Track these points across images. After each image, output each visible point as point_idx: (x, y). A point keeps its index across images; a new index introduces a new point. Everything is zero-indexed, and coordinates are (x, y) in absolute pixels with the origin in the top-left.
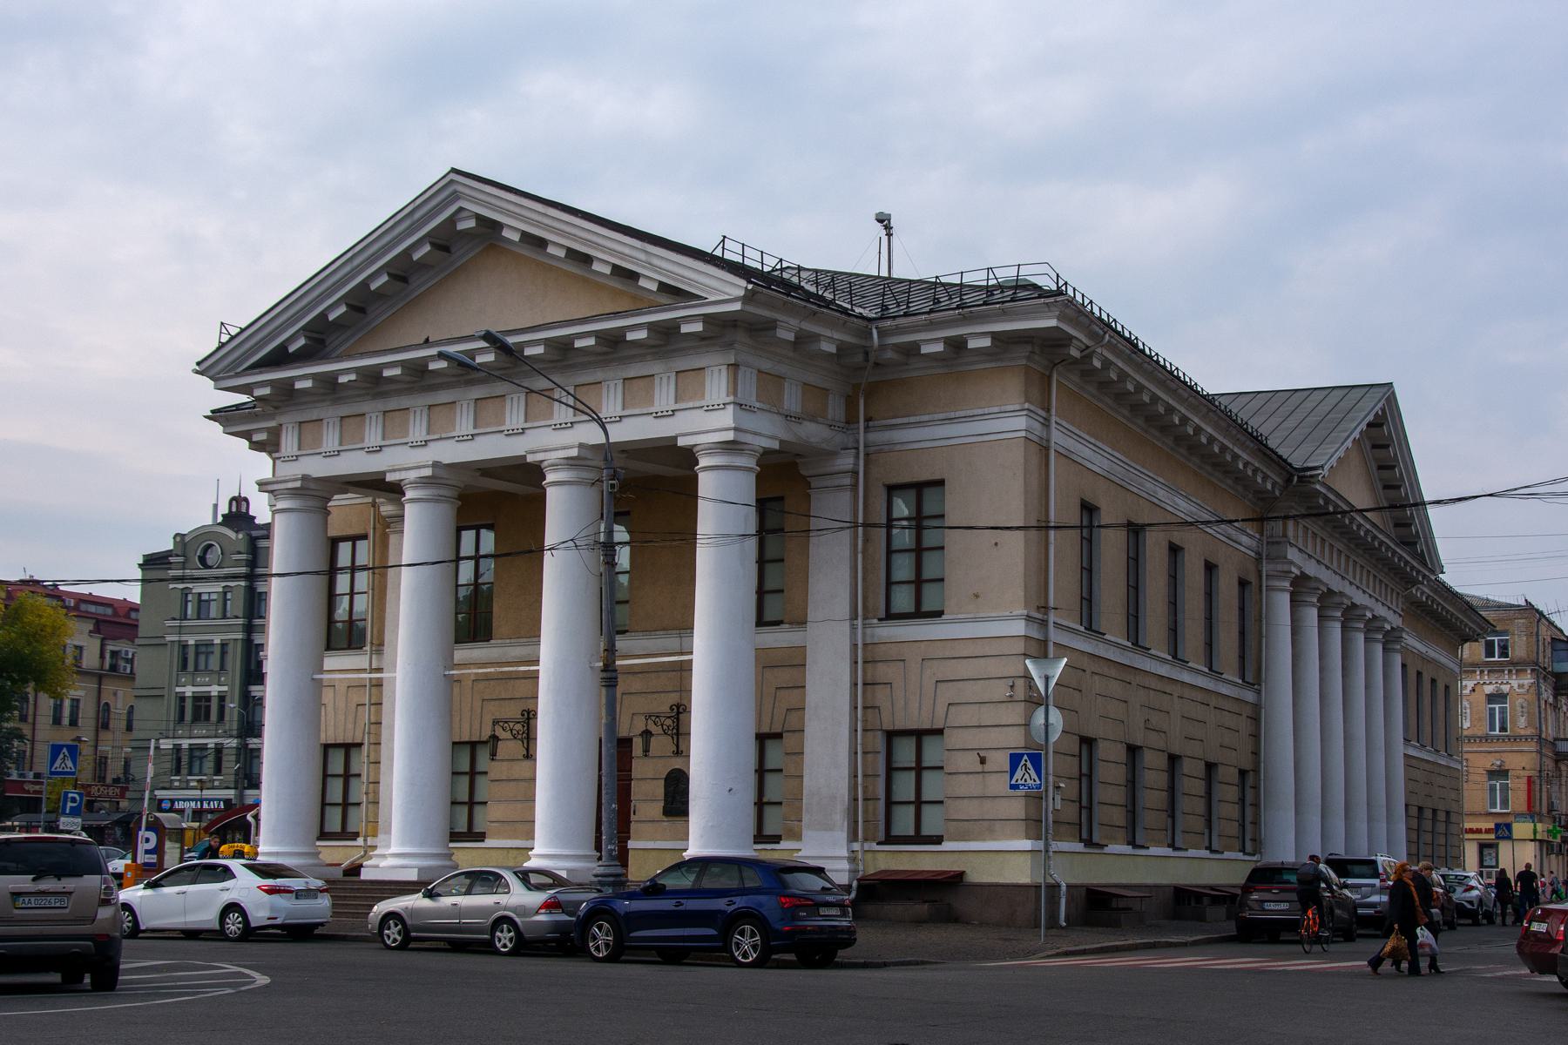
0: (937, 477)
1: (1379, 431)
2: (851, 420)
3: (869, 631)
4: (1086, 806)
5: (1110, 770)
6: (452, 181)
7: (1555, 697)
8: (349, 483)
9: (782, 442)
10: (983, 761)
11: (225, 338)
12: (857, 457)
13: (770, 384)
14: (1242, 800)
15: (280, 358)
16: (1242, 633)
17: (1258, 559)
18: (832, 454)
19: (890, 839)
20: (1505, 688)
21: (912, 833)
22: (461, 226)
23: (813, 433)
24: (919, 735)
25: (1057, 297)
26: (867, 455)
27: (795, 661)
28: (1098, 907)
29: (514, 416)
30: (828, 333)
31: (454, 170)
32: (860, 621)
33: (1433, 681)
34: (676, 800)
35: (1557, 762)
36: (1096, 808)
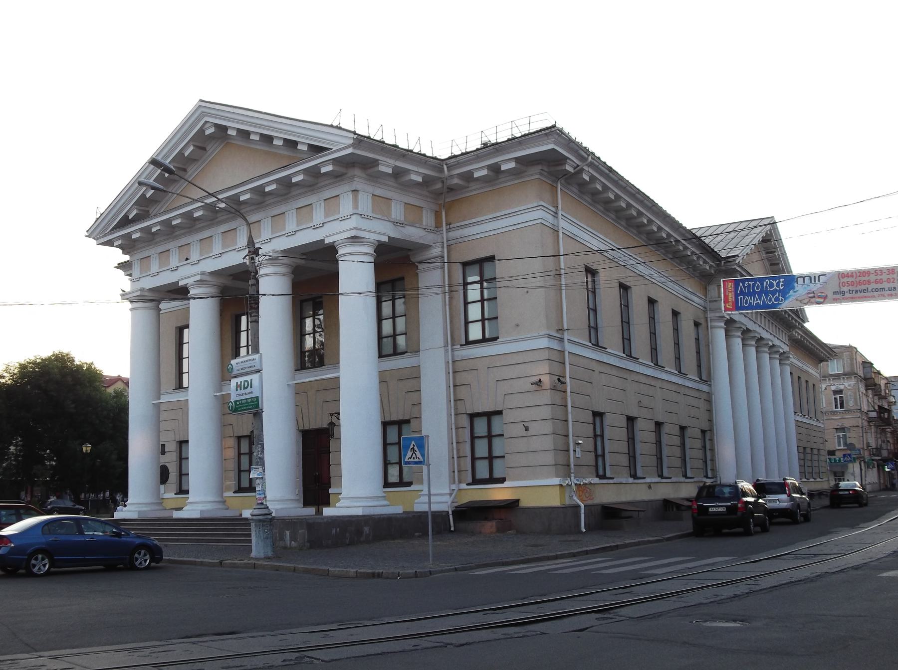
0: (491, 254)
1: (769, 245)
2: (438, 225)
3: (456, 353)
4: (599, 456)
5: (615, 430)
7: (866, 390)
8: (169, 291)
9: (389, 238)
10: (527, 429)
11: (98, 215)
12: (443, 247)
13: (381, 204)
14: (704, 447)
15: (125, 222)
16: (698, 353)
17: (705, 311)
18: (427, 247)
19: (475, 481)
20: (842, 387)
21: (488, 477)
22: (207, 132)
23: (413, 234)
24: (489, 415)
25: (553, 132)
26: (448, 246)
27: (415, 375)
28: (609, 516)
30: (415, 169)
32: (450, 347)
33: (807, 381)
35: (869, 422)
36: (607, 456)
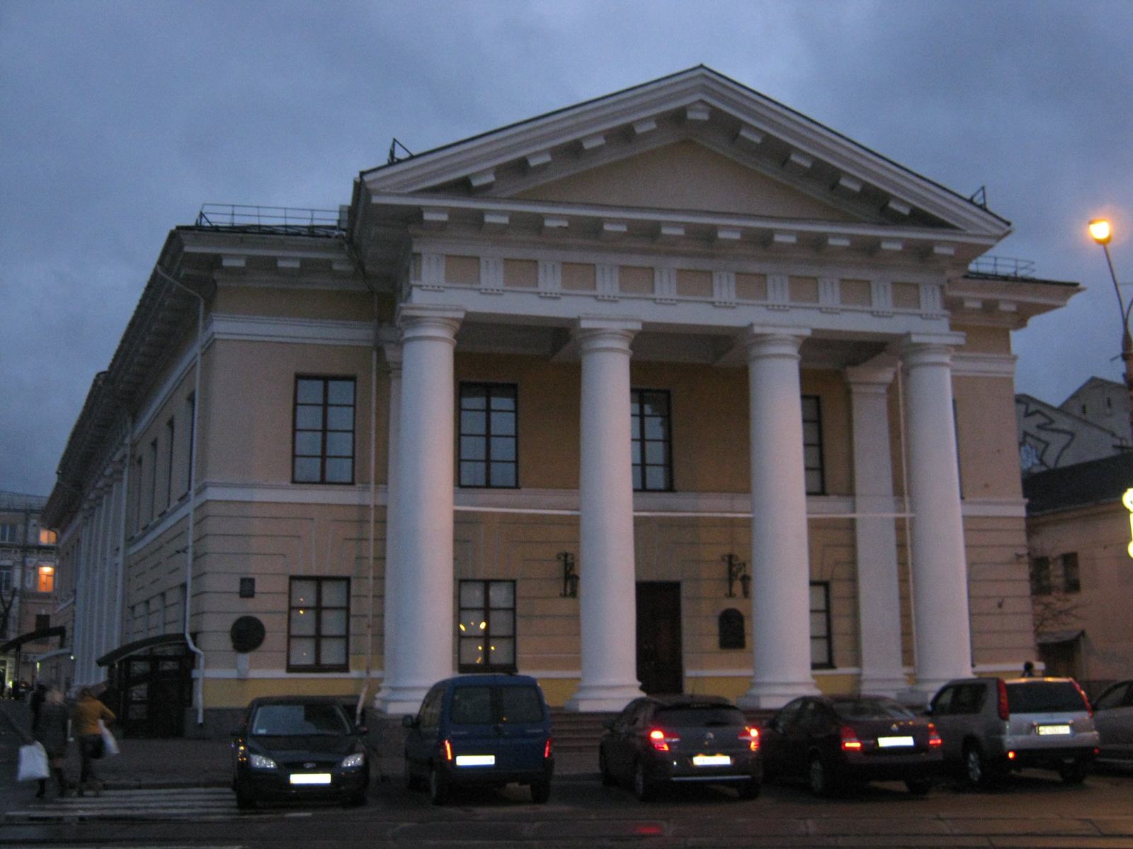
29: (725, 290)
31: (702, 66)
34: (733, 631)
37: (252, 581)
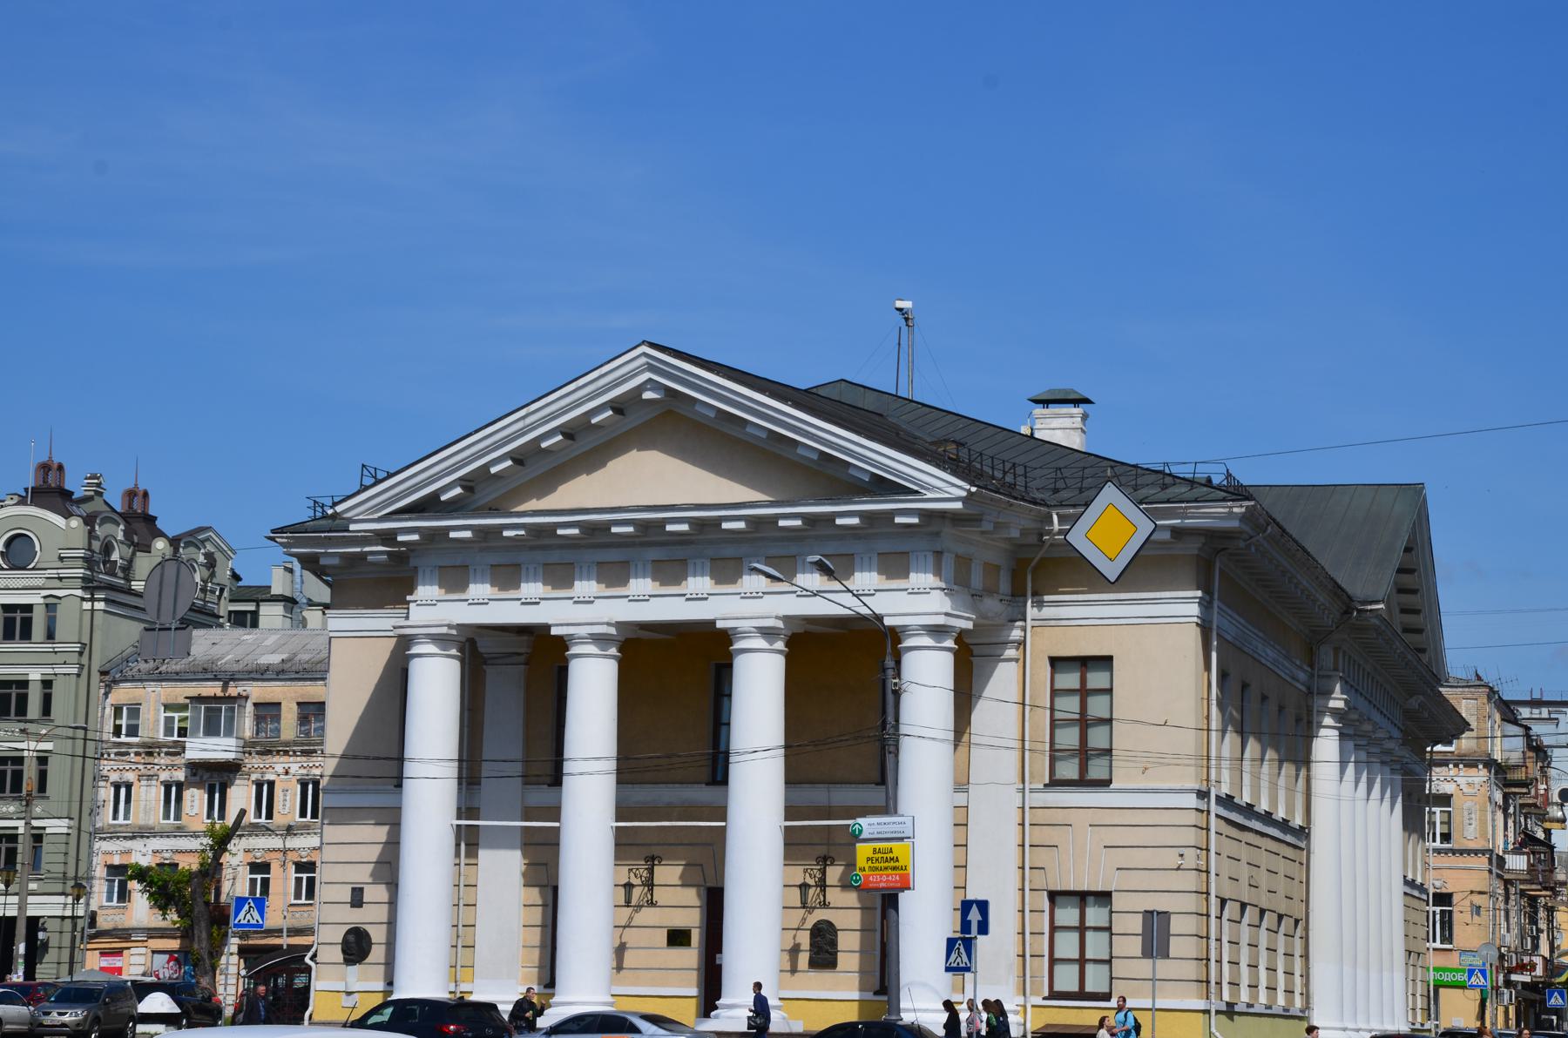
6: (645, 354)
19: (1054, 995)
21: (1076, 989)
37: (362, 890)
